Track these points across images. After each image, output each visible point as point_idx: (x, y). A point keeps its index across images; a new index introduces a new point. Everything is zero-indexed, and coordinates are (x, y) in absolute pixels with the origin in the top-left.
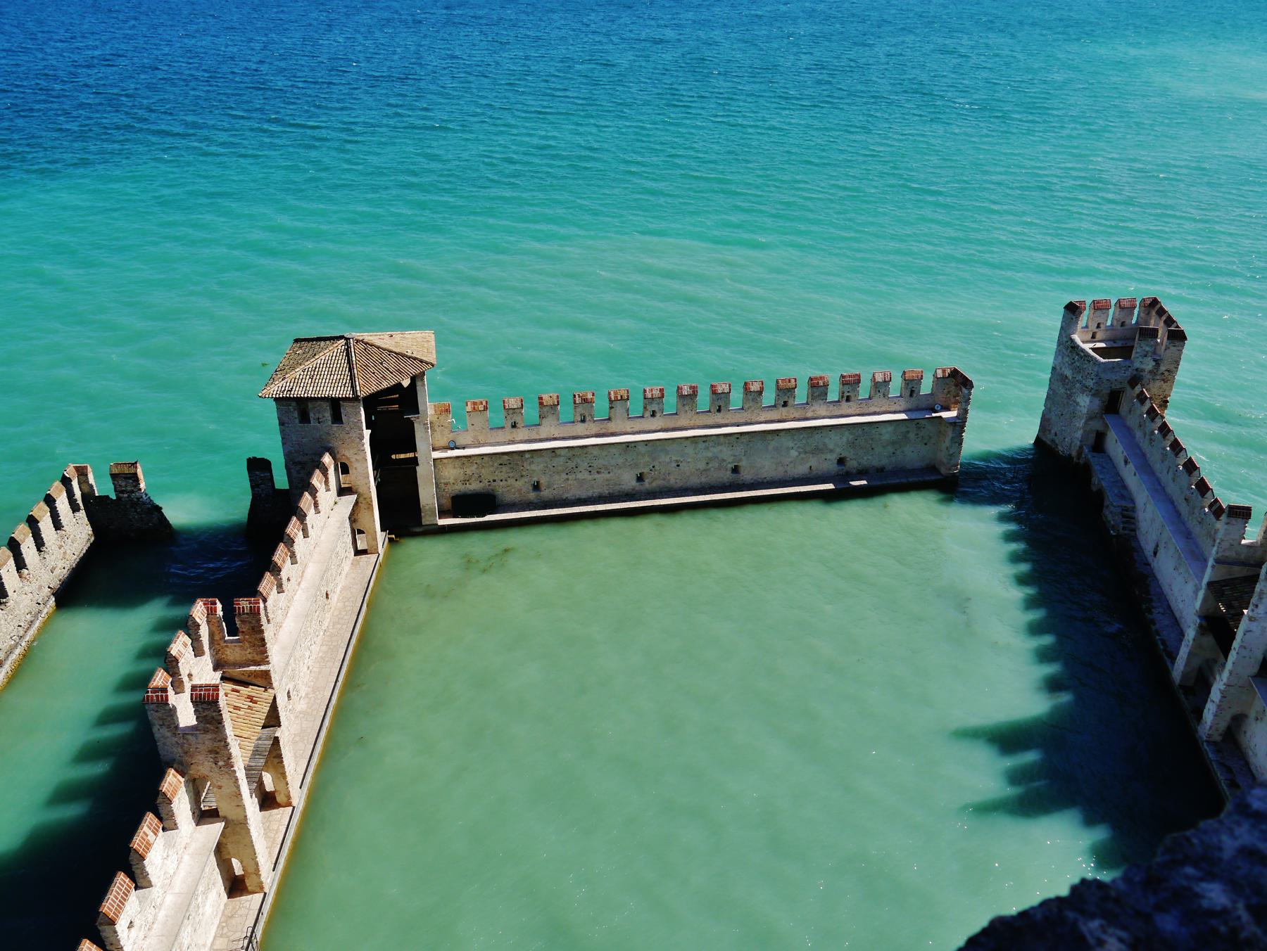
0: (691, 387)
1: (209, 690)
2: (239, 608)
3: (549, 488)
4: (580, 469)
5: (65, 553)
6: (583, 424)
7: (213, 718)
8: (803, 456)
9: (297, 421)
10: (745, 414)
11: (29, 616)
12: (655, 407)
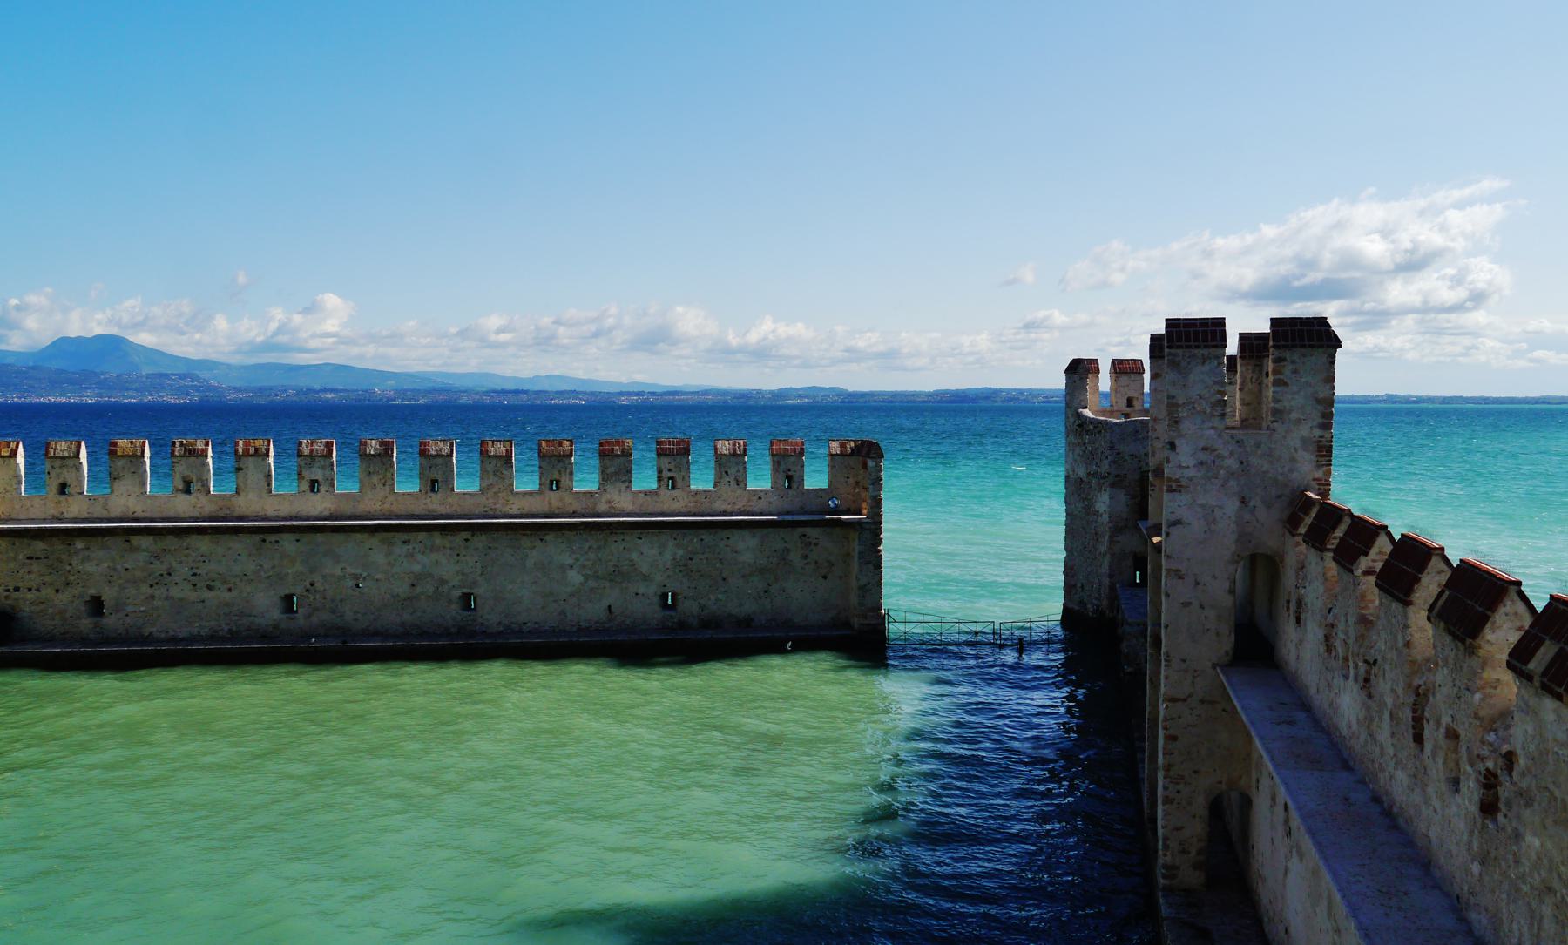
3: (117, 611)
8: (592, 583)
10: (483, 500)
12: (317, 474)
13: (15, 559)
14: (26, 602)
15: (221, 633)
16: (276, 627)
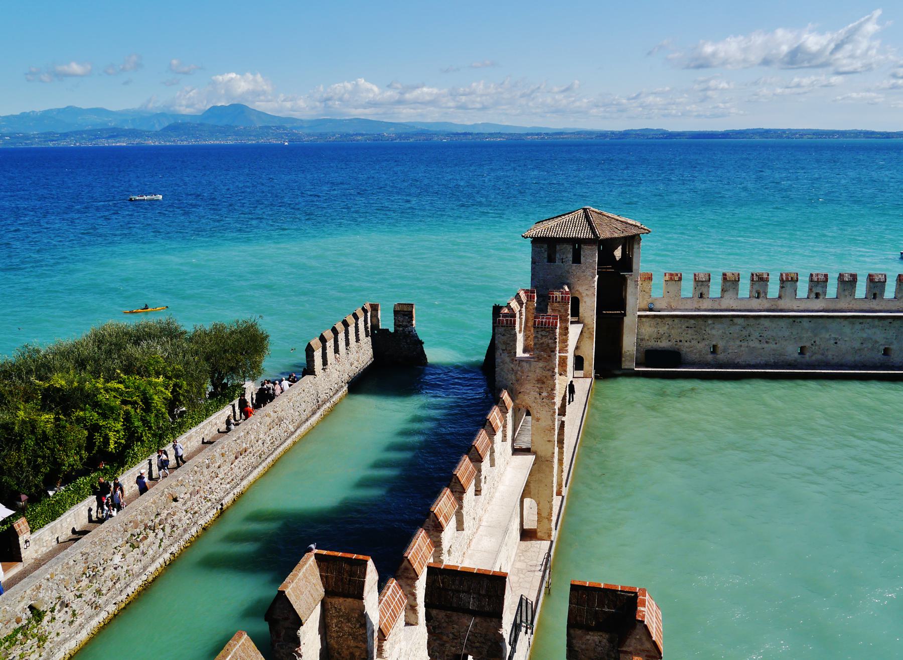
0: (851, 275)
1: (550, 319)
2: (553, 297)
3: (724, 352)
4: (752, 338)
5: (359, 358)
6: (756, 300)
7: (548, 345)
9: (546, 260)
11: (336, 385)
13: (681, 328)
14: (685, 348)
15: (770, 363)
16: (795, 361)
